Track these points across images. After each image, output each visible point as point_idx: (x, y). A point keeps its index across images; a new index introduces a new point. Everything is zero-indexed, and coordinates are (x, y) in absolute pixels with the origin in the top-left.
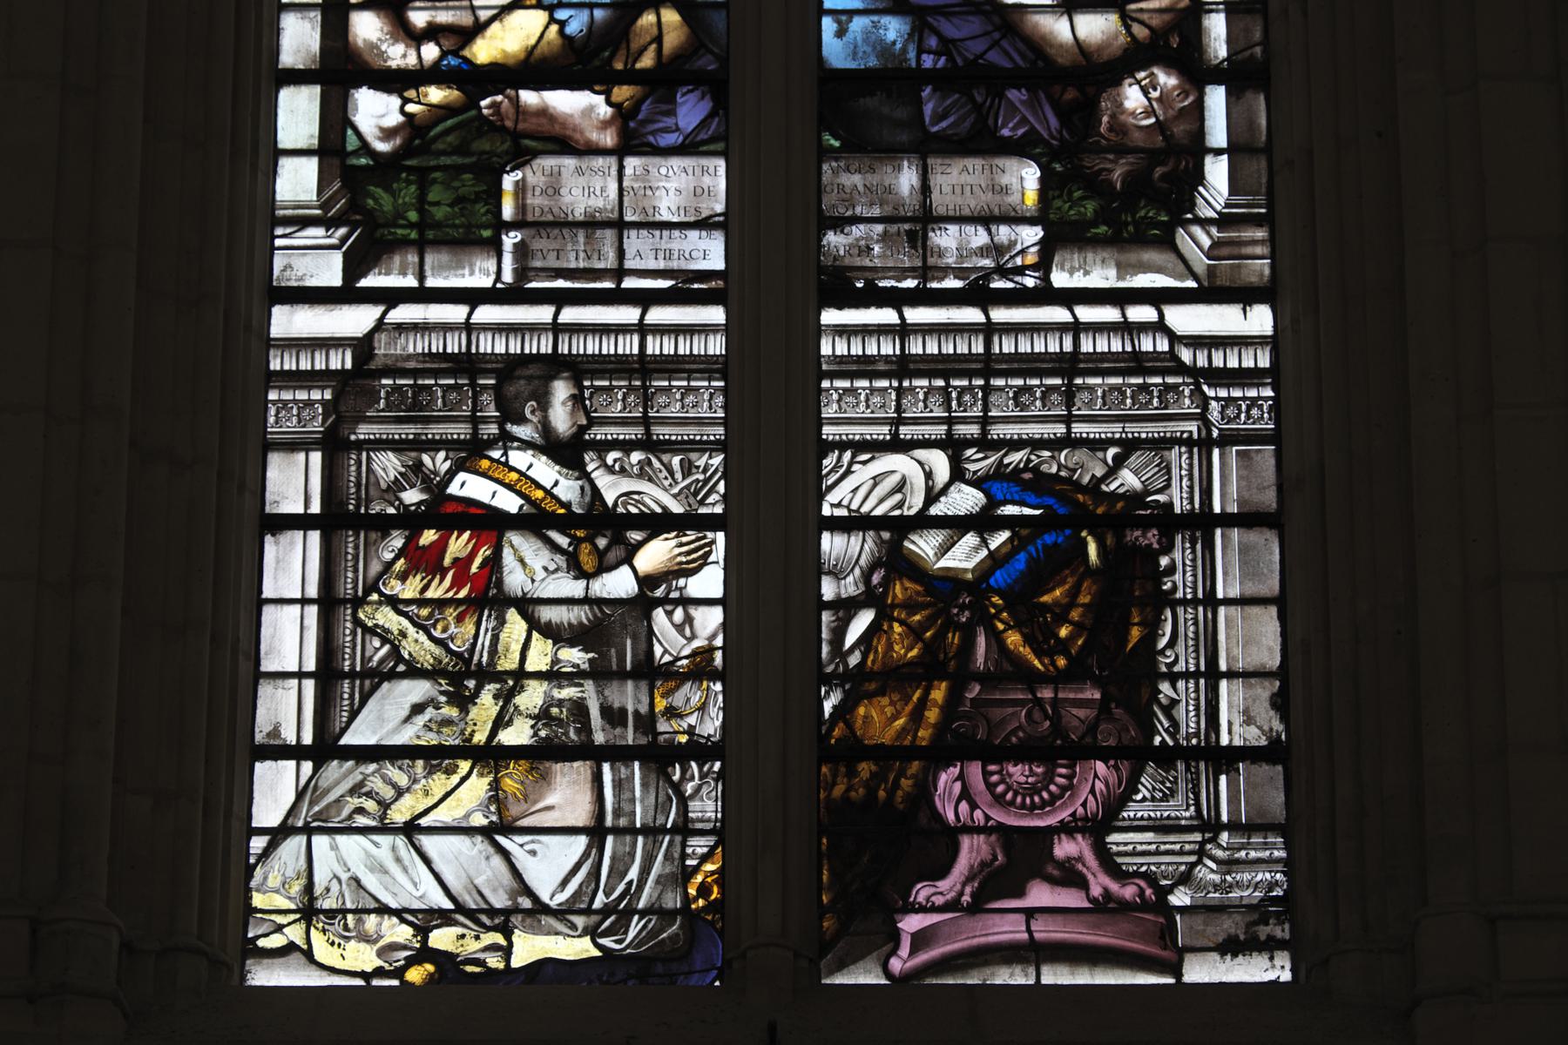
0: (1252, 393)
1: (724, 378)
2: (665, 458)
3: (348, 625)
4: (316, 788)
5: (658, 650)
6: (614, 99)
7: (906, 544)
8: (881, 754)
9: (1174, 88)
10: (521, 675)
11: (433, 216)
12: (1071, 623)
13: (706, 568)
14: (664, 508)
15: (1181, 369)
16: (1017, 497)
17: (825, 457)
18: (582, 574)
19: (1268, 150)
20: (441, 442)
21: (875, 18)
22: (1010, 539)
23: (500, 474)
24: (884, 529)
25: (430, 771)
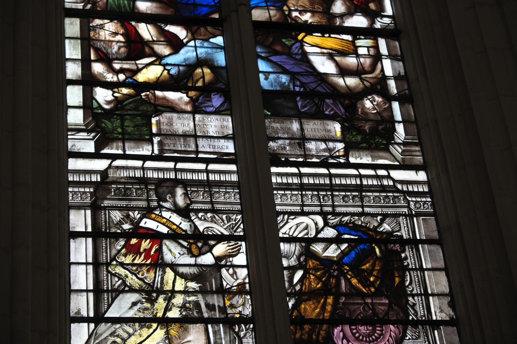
0: (424, 200)
1: (239, 189)
2: (220, 215)
3: (105, 272)
4: (96, 334)
5: (225, 284)
6: (189, 95)
7: (311, 247)
8: (312, 322)
9: (381, 102)
10: (173, 292)
11: (127, 131)
12: (374, 276)
13: (239, 254)
14: (222, 233)
15: (398, 191)
16: (348, 232)
17: (278, 217)
18: (193, 256)
19: (416, 122)
20: (136, 207)
22: (348, 247)
23: (159, 219)
24: (303, 242)
25: (141, 328)
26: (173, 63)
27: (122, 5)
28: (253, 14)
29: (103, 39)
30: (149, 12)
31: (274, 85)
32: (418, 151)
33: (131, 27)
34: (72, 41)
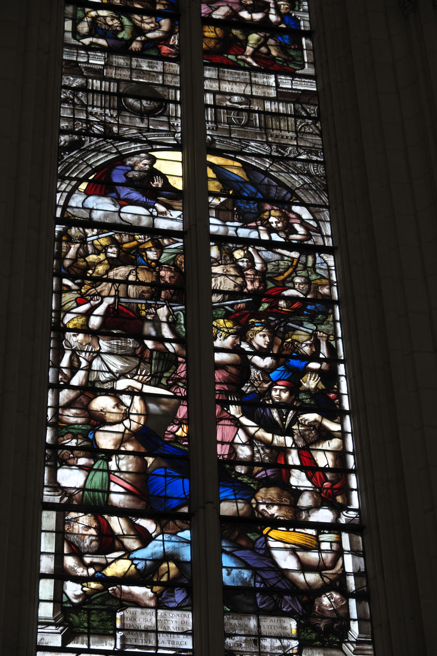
6: (154, 590)
9: (339, 599)
11: (92, 625)
19: (371, 620)
21: (240, 570)
26: (140, 557)
27: (97, 498)
28: (221, 508)
29: (77, 532)
30: (122, 505)
31: (236, 580)
32: (370, 650)
33: (103, 520)
34: (48, 534)
